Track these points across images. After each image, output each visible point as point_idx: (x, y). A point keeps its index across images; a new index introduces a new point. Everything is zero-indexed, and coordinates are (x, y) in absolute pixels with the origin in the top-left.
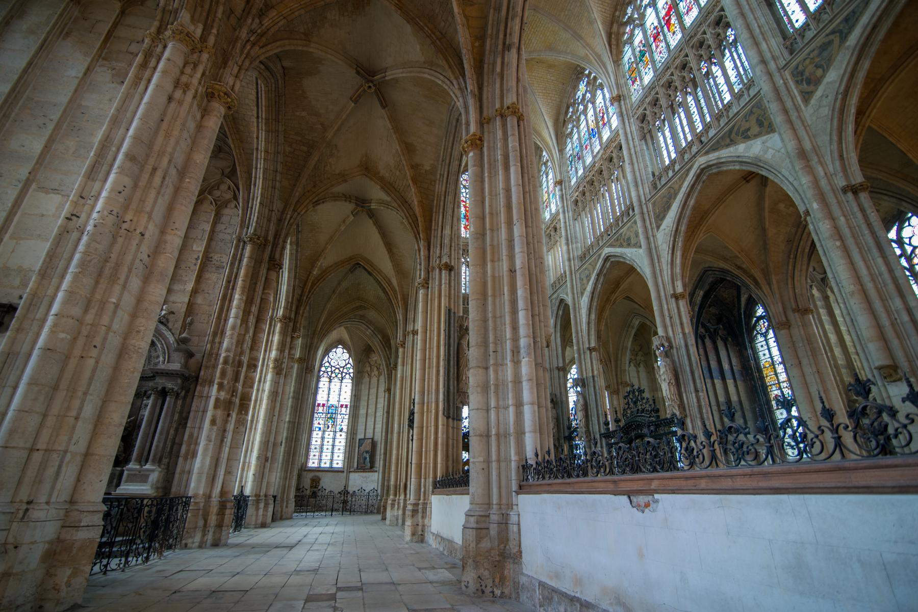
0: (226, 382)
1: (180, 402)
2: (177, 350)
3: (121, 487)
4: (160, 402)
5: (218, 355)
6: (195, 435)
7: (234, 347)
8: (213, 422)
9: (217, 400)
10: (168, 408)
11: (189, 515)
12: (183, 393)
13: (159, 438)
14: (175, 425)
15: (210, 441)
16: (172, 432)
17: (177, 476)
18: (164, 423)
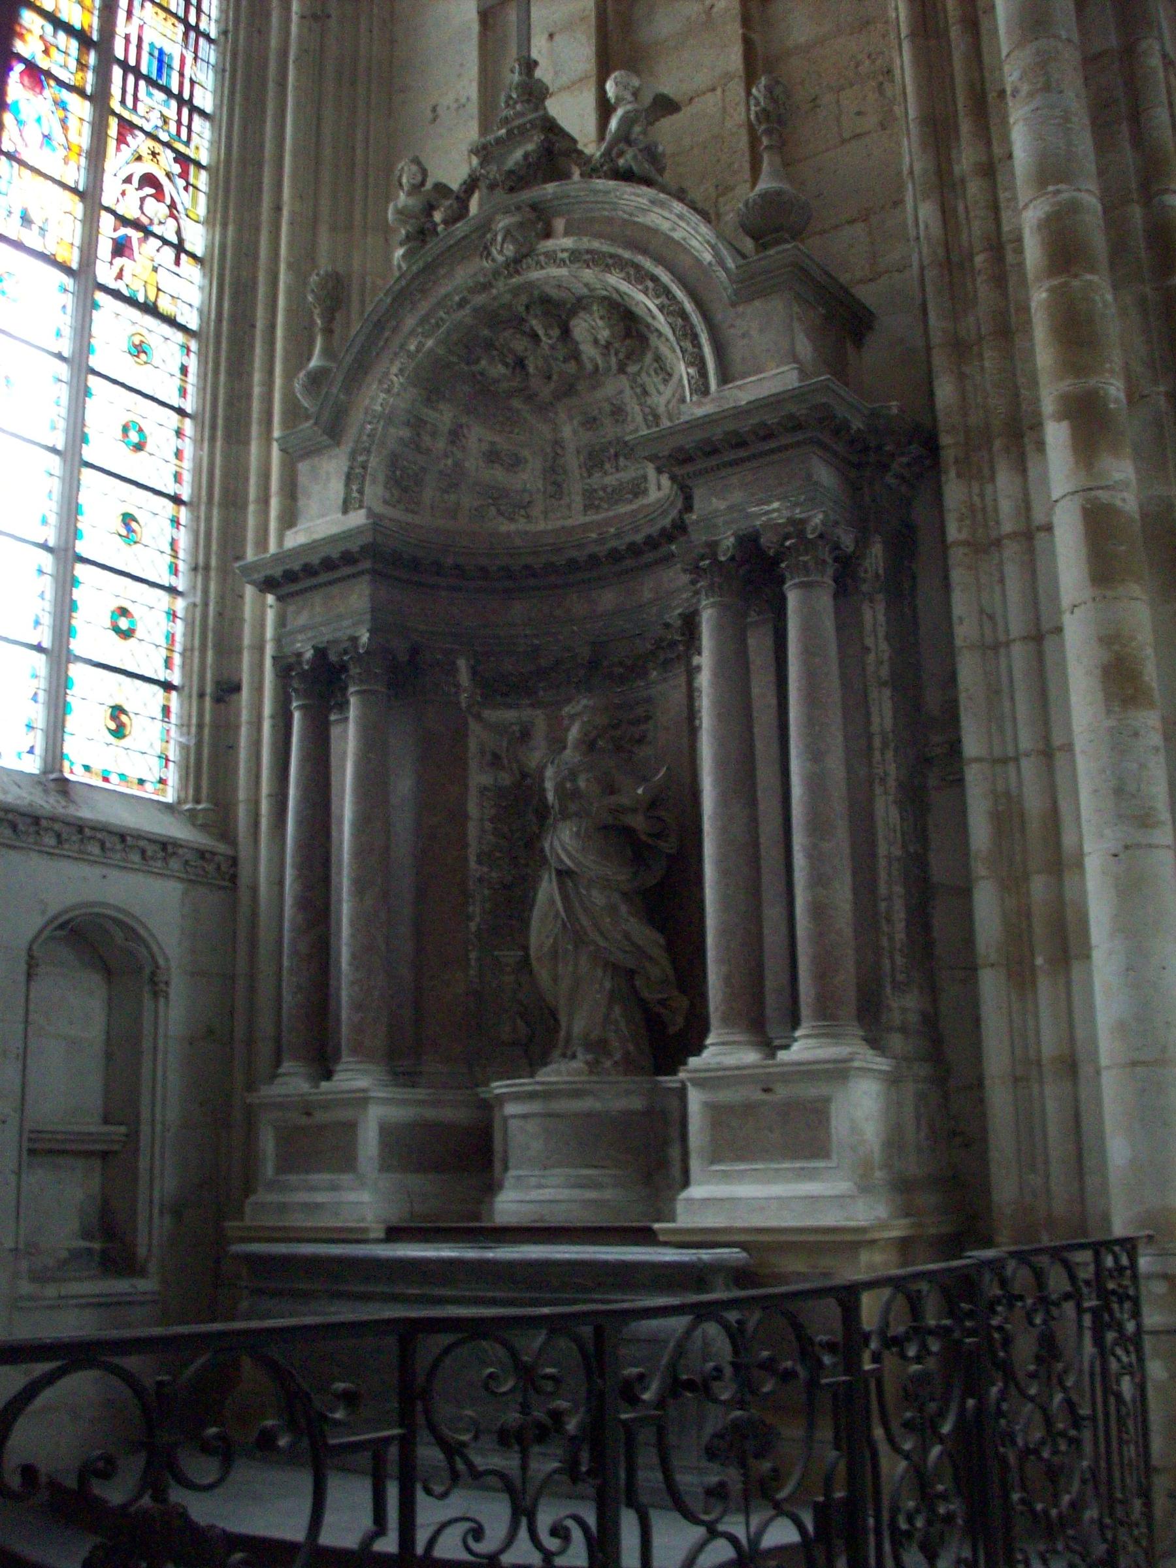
0: (1115, 389)
1: (874, 616)
2: (750, 287)
3: (696, 1191)
4: (759, 644)
5: (1001, 247)
6: (1033, 803)
7: (1084, 144)
8: (1121, 680)
9: (1099, 522)
10: (808, 652)
11: (1156, 1369)
12: (876, 556)
13: (815, 857)
14: (890, 767)
15: (1145, 820)
16: (887, 812)
17: (1000, 1099)
18: (815, 755)
